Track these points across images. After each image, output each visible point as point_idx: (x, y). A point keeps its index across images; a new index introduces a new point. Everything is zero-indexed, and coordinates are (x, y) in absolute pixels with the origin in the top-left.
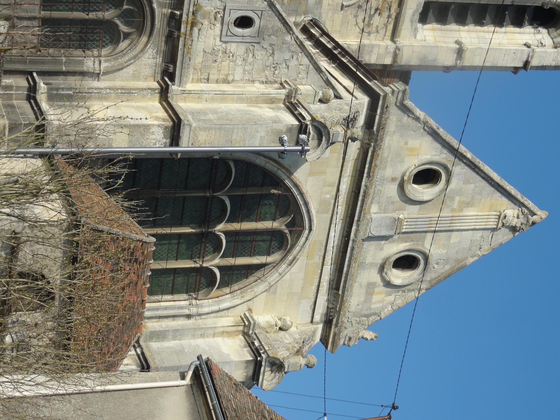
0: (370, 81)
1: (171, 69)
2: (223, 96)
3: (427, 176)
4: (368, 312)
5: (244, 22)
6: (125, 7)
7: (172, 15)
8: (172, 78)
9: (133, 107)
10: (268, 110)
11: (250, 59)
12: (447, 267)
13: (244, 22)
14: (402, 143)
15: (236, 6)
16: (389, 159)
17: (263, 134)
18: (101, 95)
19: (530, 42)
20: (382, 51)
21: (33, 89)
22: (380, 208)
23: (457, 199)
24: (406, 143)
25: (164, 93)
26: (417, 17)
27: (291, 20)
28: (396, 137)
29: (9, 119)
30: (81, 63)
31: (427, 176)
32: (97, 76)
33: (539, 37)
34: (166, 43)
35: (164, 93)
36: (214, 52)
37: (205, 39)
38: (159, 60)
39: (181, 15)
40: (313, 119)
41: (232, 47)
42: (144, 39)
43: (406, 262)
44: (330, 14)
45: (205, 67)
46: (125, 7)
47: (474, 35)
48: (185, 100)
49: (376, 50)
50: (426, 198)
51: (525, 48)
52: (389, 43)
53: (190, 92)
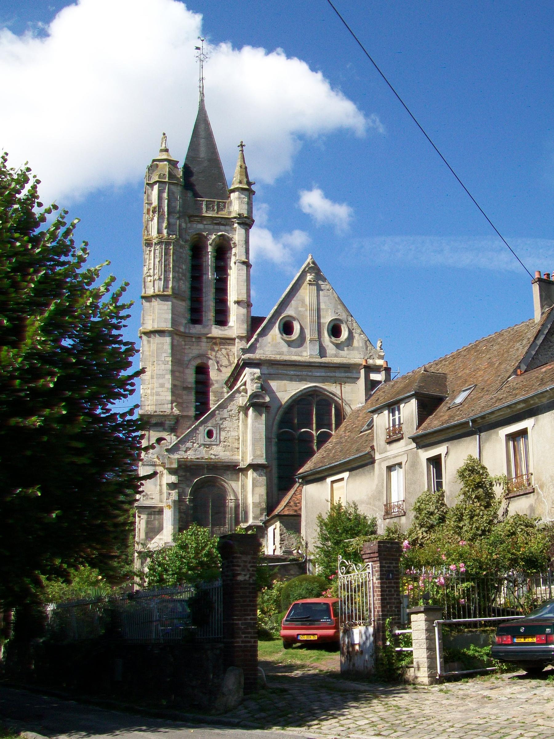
2: (244, 441)
3: (287, 328)
4: (365, 347)
5: (210, 434)
11: (228, 429)
12: (339, 307)
13: (210, 434)
14: (269, 345)
15: (202, 439)
16: (278, 350)
17: (257, 424)
18: (245, 498)
22: (305, 351)
23: (300, 309)
24: (269, 343)
26: (223, 328)
27: (226, 396)
28: (266, 349)
30: (231, 508)
31: (287, 328)
32: (237, 500)
36: (225, 447)
37: (219, 453)
43: (335, 331)
44: (223, 375)
45: (232, 450)
48: (246, 460)
50: (299, 327)
53: (243, 457)
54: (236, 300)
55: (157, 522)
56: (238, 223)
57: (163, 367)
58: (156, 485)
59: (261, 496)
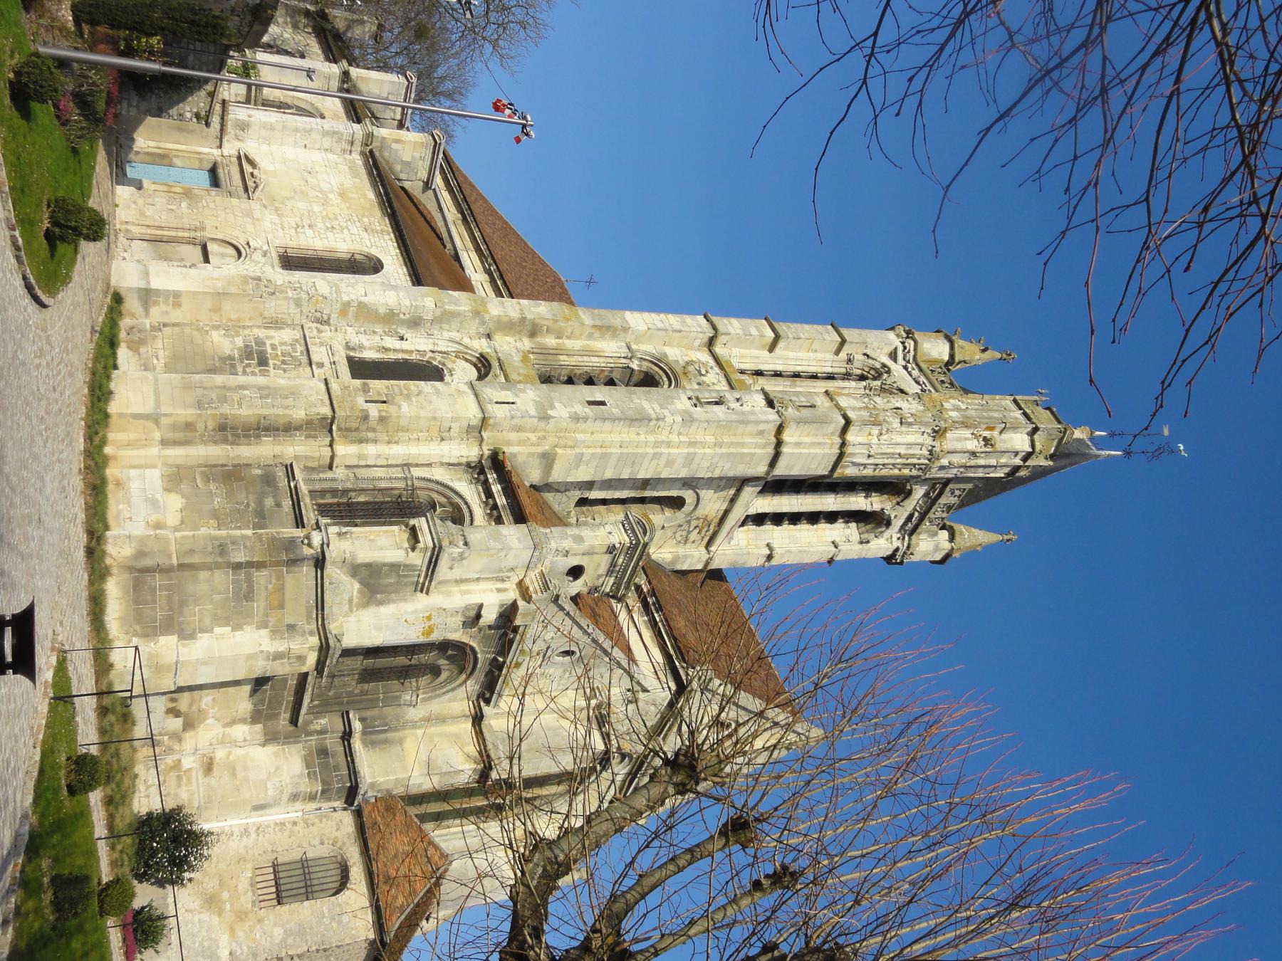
1: (488, 695)
6: (450, 652)
7: (495, 659)
8: (488, 702)
9: (446, 736)
19: (837, 540)
20: (695, 560)
21: (347, 735)
25: (478, 719)
29: (323, 781)
33: (848, 531)
34: (486, 676)
35: (478, 719)
38: (477, 687)
39: (504, 662)
40: (619, 748)
41: (551, 671)
42: (464, 676)
46: (450, 652)
47: (786, 534)
49: (689, 561)
51: (832, 549)
52: (703, 550)
54: (778, 552)
55: (392, 581)
56: (897, 549)
57: (706, 464)
58: (481, 571)
59: (420, 785)
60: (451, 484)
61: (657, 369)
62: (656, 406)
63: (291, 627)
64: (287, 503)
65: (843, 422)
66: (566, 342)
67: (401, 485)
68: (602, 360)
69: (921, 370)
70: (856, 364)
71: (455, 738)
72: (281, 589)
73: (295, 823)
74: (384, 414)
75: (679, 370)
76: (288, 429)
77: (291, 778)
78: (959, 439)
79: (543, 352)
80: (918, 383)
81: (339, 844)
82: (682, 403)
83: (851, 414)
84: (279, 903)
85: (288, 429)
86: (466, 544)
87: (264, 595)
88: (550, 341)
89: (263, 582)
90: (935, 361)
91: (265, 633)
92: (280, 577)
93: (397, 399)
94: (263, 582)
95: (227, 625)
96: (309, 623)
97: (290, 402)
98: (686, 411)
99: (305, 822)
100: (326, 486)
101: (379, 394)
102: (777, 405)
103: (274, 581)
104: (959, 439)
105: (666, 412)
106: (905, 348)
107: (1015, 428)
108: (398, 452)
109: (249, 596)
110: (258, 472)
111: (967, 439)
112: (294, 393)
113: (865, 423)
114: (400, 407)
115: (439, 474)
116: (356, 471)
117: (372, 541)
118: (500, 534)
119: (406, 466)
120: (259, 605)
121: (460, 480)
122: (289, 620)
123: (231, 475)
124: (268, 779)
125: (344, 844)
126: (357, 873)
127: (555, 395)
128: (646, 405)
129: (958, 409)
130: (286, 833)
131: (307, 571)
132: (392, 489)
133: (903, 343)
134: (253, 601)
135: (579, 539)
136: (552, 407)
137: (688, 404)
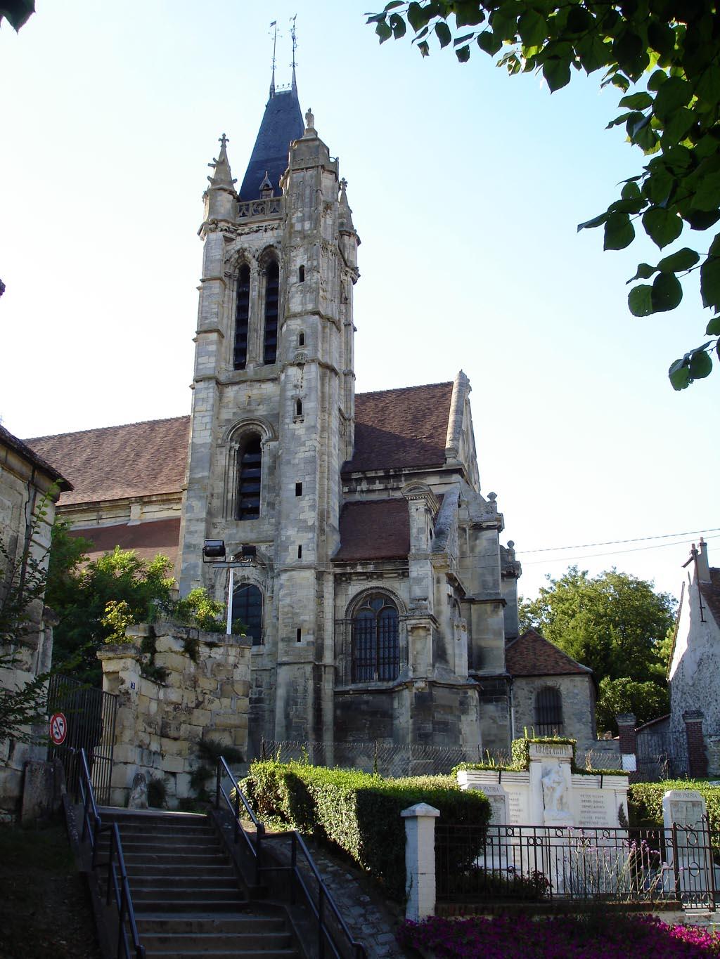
0: (442, 467)
10: (478, 541)
60: (351, 597)
61: (241, 430)
62: (303, 449)
63: (462, 703)
64: (365, 697)
65: (317, 317)
66: (216, 491)
67: (350, 627)
68: (231, 468)
69: (245, 224)
70: (231, 271)
71: (480, 617)
72: (443, 707)
73: (517, 712)
74: (311, 632)
75: (245, 416)
76: (318, 692)
77: (497, 711)
78: (325, 229)
79: (224, 511)
80: (257, 231)
81: (532, 690)
82: (300, 429)
83: (310, 307)
84: (562, 723)
85: (318, 692)
86: (425, 600)
87: (446, 716)
88: (217, 503)
89: (439, 716)
90: (234, 207)
91: (463, 718)
92: (437, 706)
93: (296, 620)
94: (439, 716)
95: (459, 737)
96: (459, 694)
97: (300, 688)
98: (308, 429)
99: (516, 706)
100: (349, 673)
101: (293, 632)
102: (303, 362)
103: (439, 710)
104: (325, 229)
105: (308, 443)
106: (226, 230)
107: (319, 182)
108: (329, 626)
109: (446, 723)
110: (338, 712)
111: (325, 222)
112: (292, 685)
113: (316, 301)
114: (305, 621)
115: (343, 602)
116: (337, 653)
117: (417, 653)
118: (414, 578)
119: (336, 622)
120: (450, 718)
121: (347, 590)
122: (457, 704)
123: (341, 731)
124: (497, 723)
125: (532, 687)
126: (550, 682)
127: (292, 516)
128: (301, 455)
129: (302, 220)
130: (522, 716)
131: (437, 692)
132: (352, 633)
133: (222, 230)
134: (448, 723)
135: (421, 530)
136: (305, 521)
137: (298, 425)
